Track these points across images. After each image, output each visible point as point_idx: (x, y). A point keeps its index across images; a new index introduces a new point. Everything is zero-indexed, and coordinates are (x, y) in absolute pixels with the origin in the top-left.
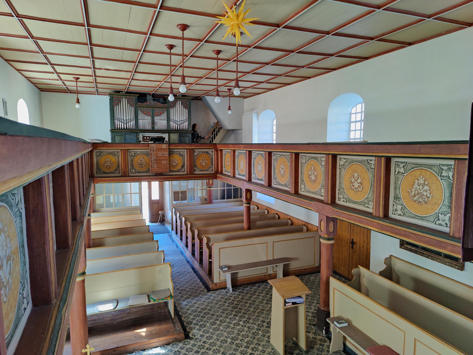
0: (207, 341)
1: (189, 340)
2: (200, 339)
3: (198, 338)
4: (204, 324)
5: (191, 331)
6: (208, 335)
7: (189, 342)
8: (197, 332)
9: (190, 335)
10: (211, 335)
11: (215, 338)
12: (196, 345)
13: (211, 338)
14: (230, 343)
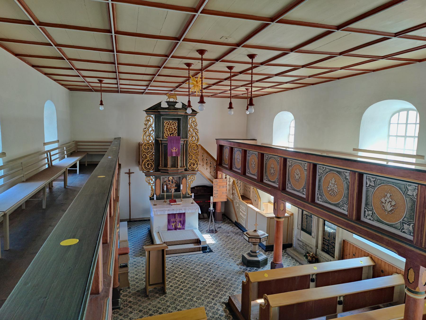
0: (211, 300)
1: (225, 301)
2: (216, 302)
3: (218, 303)
4: (214, 315)
5: (225, 309)
6: (211, 305)
7: (225, 300)
8: (219, 308)
9: (224, 305)
10: (208, 304)
11: (205, 302)
12: (219, 298)
13: (208, 302)
14: (194, 297)
